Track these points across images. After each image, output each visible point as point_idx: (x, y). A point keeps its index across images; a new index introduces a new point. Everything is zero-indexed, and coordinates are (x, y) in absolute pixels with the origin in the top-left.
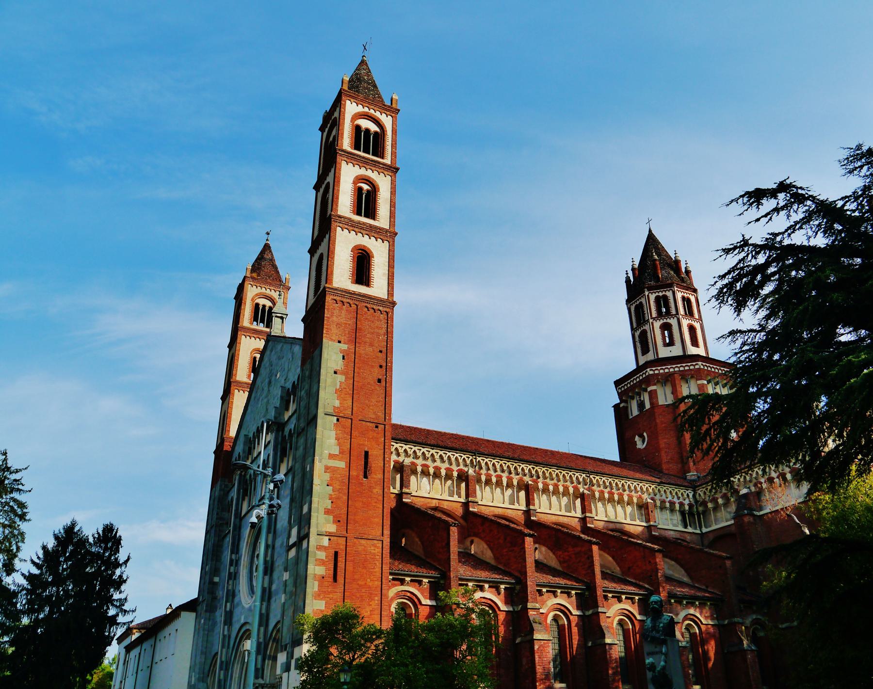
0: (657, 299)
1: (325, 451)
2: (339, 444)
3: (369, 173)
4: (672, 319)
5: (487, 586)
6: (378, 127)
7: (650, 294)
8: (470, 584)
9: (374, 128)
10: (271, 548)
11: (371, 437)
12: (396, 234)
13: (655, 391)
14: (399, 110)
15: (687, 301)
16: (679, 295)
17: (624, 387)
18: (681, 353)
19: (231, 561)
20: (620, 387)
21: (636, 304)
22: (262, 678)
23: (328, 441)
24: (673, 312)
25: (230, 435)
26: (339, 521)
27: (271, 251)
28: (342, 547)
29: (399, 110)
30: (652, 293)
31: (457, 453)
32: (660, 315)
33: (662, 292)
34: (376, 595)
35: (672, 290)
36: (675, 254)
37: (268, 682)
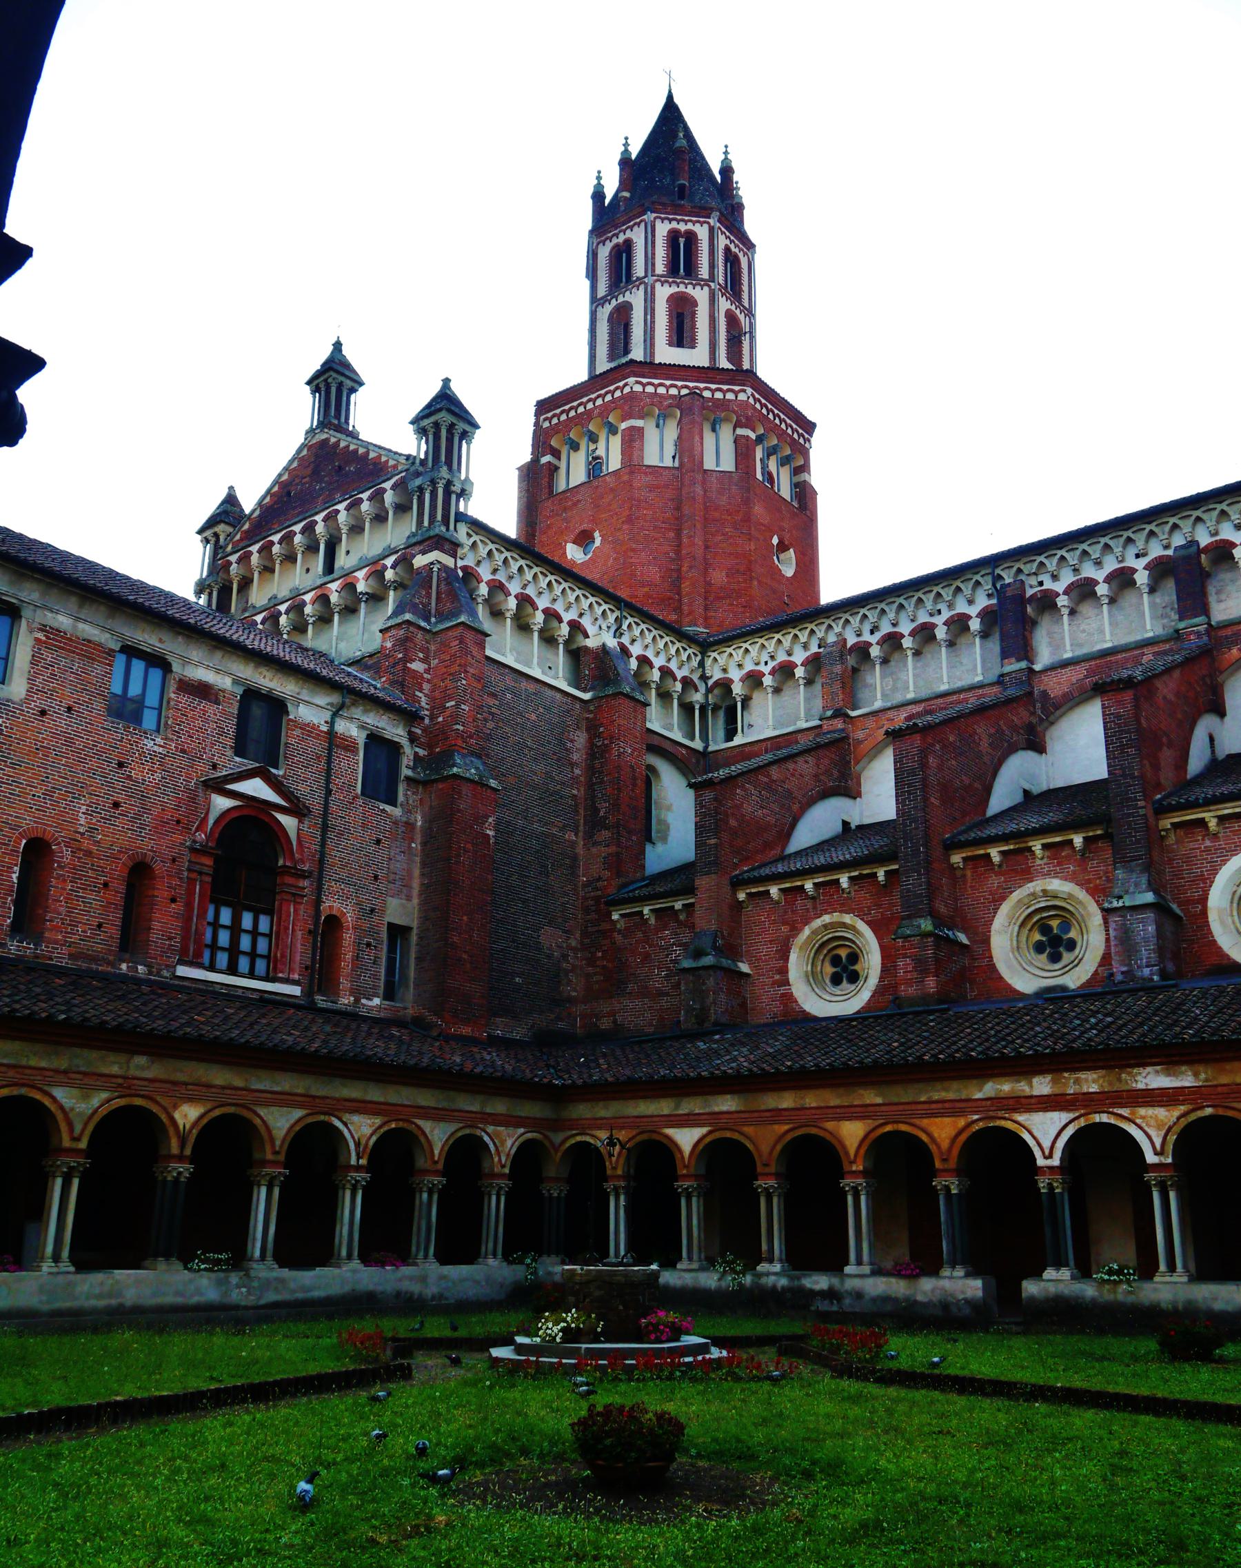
0: (673, 236)
4: (698, 288)
7: (658, 223)
13: (640, 431)
15: (732, 260)
16: (722, 242)
17: (558, 416)
18: (707, 364)
20: (549, 415)
21: (615, 241)
24: (704, 272)
30: (663, 220)
32: (673, 269)
33: (686, 222)
35: (708, 223)
36: (726, 153)
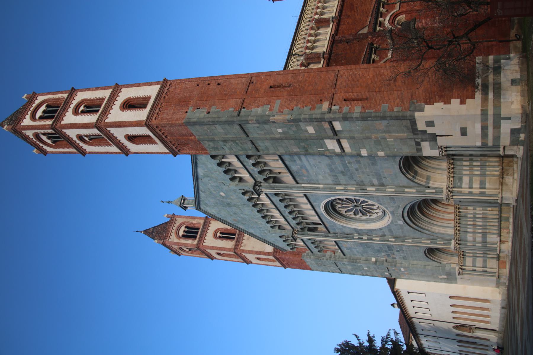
1: (267, 114)
2: (263, 104)
3: (72, 106)
5: (381, 19)
6: (43, 104)
8: (378, 28)
9: (43, 108)
10: (347, 186)
11: (260, 85)
12: (117, 84)
14: (34, 92)
19: (359, 238)
22: (442, 188)
23: (259, 113)
25: (272, 252)
26: (321, 100)
27: (148, 229)
28: (341, 97)
29: (34, 92)
31: (288, 67)
34: (380, 71)
37: (446, 184)
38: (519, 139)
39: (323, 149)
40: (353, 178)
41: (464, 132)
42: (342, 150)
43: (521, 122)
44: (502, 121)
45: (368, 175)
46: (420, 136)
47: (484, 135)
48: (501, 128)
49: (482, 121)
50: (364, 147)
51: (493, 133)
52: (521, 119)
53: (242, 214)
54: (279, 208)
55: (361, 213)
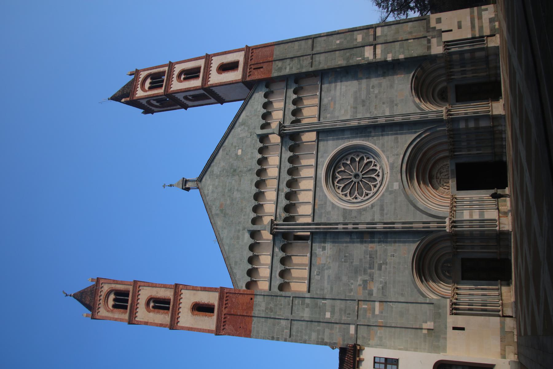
38: (495, 27)
39: (360, 58)
40: (369, 109)
41: (460, 27)
42: (375, 55)
43: (494, 12)
44: (483, 12)
45: (384, 103)
46: (431, 34)
47: (473, 26)
48: (483, 18)
49: (471, 14)
50: (391, 52)
51: (479, 23)
52: (493, 9)
53: (237, 190)
54: (281, 174)
55: (357, 191)
